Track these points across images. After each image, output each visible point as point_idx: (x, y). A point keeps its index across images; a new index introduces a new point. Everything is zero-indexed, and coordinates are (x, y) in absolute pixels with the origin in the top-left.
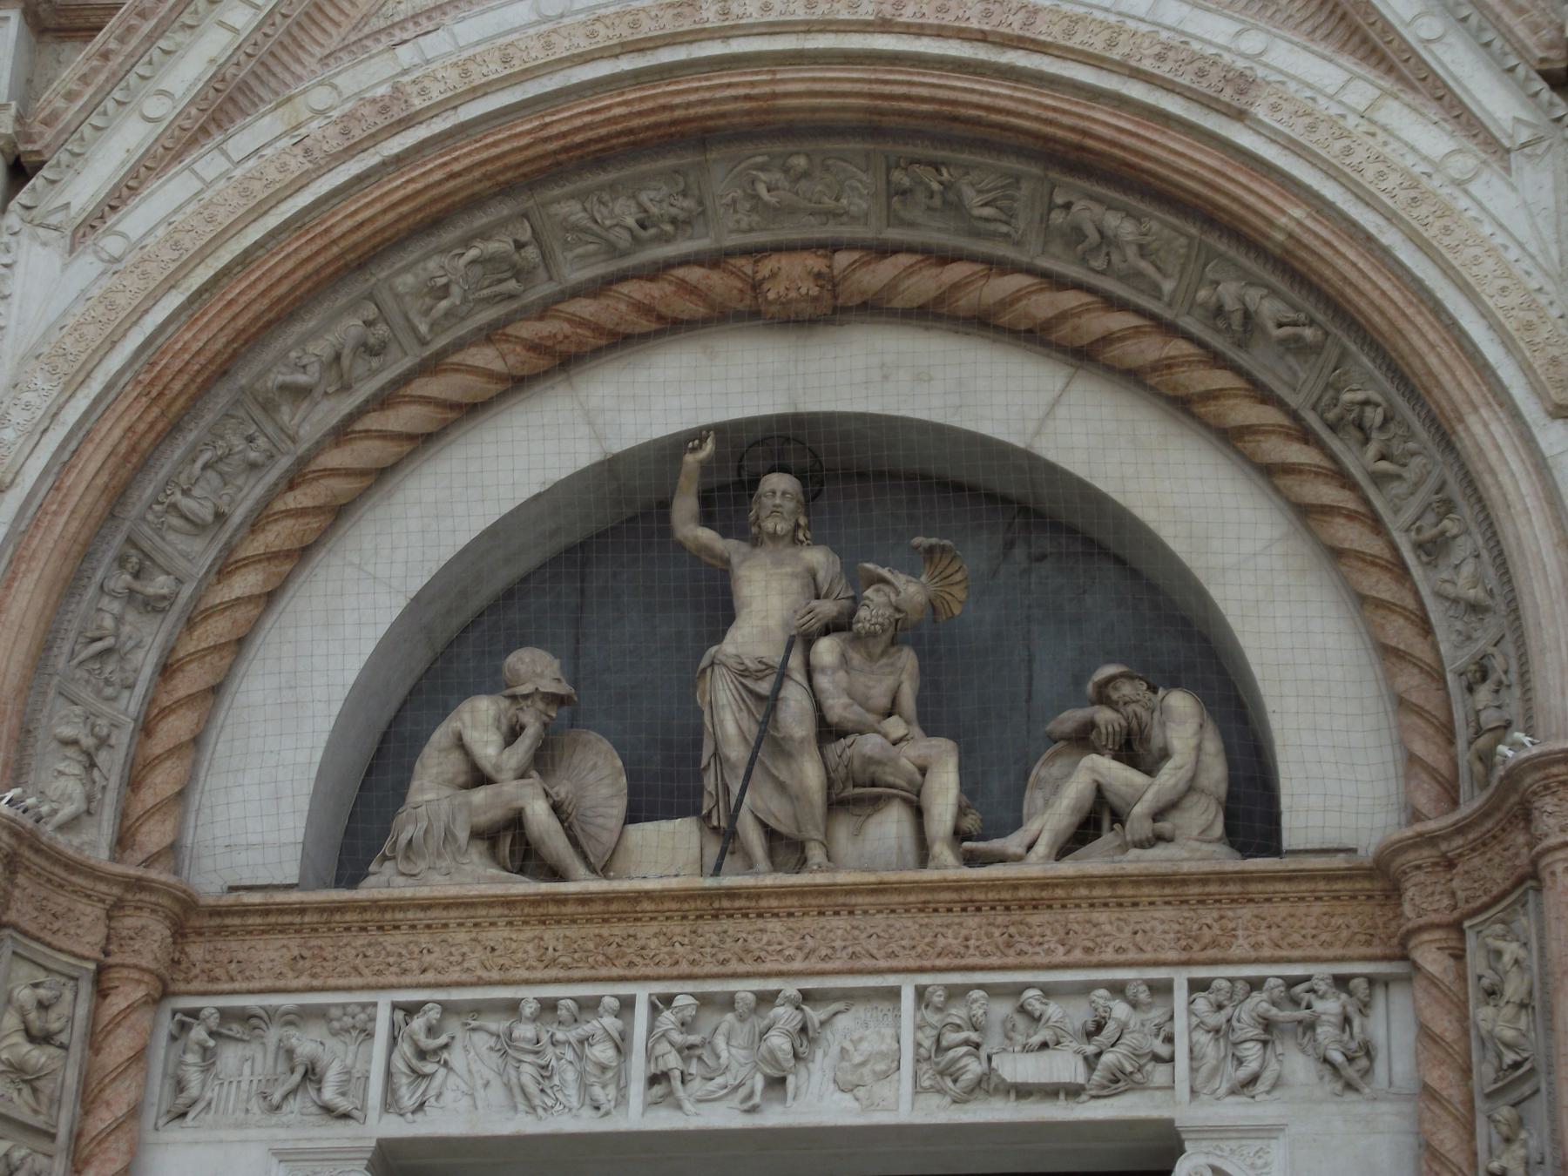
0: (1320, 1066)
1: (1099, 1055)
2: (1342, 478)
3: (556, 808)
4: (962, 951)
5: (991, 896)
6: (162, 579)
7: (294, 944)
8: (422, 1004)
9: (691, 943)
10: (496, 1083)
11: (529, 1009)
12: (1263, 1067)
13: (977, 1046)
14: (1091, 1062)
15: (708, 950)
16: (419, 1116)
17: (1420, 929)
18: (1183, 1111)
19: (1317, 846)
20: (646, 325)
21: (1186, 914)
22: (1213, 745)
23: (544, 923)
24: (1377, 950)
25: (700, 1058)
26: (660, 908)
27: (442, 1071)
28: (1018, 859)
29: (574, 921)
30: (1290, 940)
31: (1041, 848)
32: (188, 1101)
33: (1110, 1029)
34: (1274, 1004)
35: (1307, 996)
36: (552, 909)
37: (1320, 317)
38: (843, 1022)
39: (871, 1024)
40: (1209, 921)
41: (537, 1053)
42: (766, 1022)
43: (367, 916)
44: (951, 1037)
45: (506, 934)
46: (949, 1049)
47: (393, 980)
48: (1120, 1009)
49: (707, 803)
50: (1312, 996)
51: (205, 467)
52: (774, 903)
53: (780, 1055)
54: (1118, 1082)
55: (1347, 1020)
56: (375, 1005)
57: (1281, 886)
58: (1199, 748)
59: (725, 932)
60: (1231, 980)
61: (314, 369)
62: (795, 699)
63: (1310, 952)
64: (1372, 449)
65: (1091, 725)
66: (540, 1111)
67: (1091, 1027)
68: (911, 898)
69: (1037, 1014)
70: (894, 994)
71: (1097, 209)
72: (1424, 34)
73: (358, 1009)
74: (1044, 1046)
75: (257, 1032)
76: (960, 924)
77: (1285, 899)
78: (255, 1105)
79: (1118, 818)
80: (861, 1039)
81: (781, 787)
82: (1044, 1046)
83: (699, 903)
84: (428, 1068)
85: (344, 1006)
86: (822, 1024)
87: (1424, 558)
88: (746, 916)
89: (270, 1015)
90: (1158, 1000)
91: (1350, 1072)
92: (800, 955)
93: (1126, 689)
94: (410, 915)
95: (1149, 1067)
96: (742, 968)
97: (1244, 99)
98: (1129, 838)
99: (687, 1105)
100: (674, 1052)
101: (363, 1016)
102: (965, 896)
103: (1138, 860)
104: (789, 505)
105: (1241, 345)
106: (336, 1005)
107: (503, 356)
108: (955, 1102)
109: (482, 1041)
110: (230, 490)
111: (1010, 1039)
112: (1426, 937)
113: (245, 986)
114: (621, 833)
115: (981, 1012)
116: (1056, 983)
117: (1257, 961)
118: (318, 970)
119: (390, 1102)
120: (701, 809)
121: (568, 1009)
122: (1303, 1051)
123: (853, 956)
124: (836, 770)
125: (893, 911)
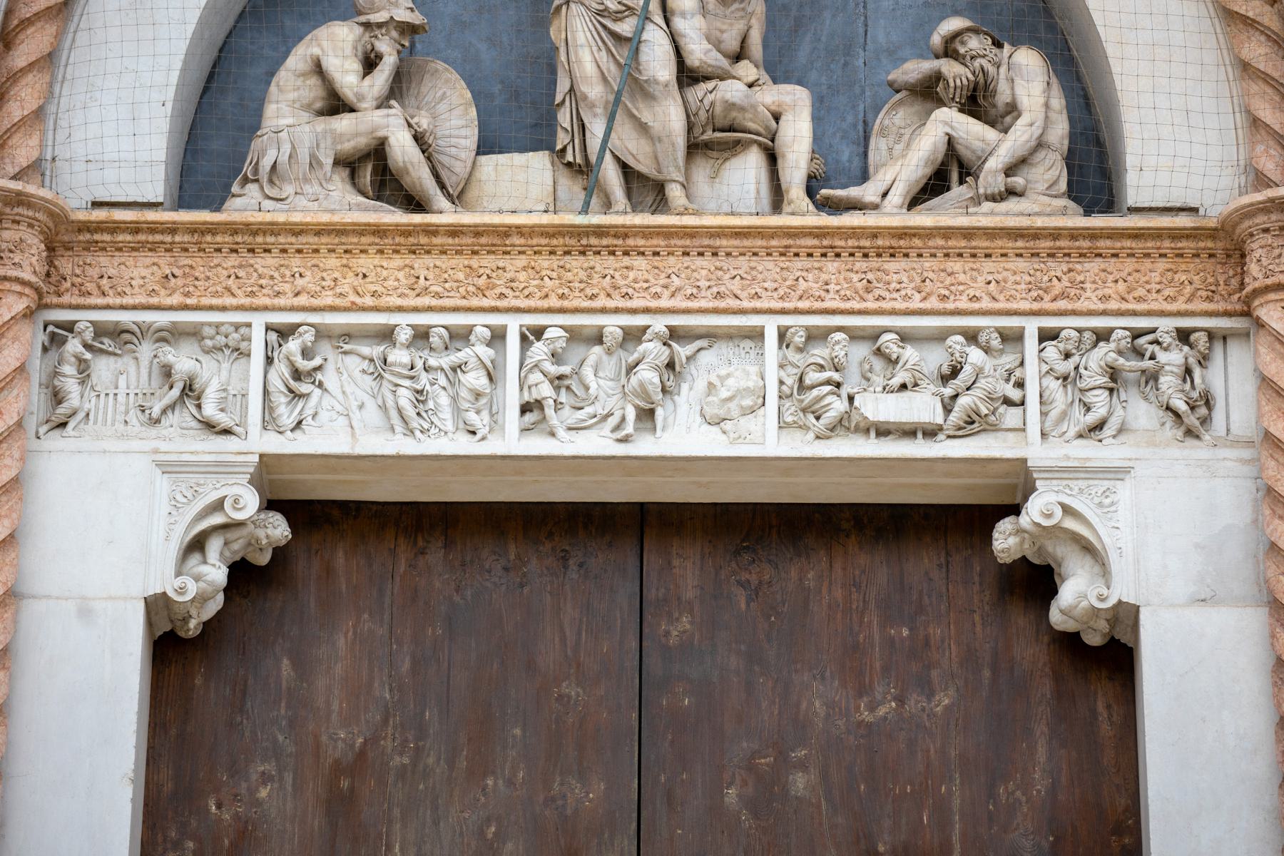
0: (1161, 413)
1: (955, 397)
3: (419, 139)
4: (823, 294)
5: (850, 243)
7: (165, 263)
9: (560, 278)
10: (371, 406)
11: (404, 335)
12: (1110, 414)
13: (838, 385)
15: (577, 285)
16: (298, 433)
18: (1037, 453)
19: (1161, 205)
21: (1036, 266)
22: (1058, 102)
23: (414, 253)
24: (1220, 306)
25: (568, 388)
26: (530, 242)
27: (318, 392)
28: (875, 207)
29: (444, 252)
30: (1136, 294)
31: (896, 197)
32: (69, 412)
33: (966, 375)
34: (1120, 353)
35: (1151, 348)
36: (424, 240)
38: (706, 358)
39: (735, 361)
40: (1059, 274)
41: (412, 378)
42: (636, 356)
43: (239, 239)
44: (812, 377)
45: (376, 262)
46: (813, 387)
47: (267, 301)
49: (562, 139)
50: (1156, 348)
52: (641, 242)
53: (650, 388)
54: (973, 424)
55: (1188, 371)
56: (249, 325)
57: (1128, 243)
58: (1047, 106)
59: (592, 268)
60: (1080, 331)
63: (1155, 306)
65: (938, 77)
66: (418, 433)
67: (946, 370)
68: (774, 243)
69: (894, 357)
70: (756, 335)
73: (232, 329)
74: (904, 387)
75: (129, 346)
76: (820, 269)
77: (1129, 255)
78: (134, 416)
79: (967, 171)
80: (728, 375)
81: (643, 128)
82: (904, 387)
83: (568, 241)
84: (304, 388)
85: (218, 326)
86: (688, 359)
88: (613, 253)
89: (142, 332)
90: (1008, 348)
91: (1192, 420)
92: (667, 293)
93: (974, 43)
94: (281, 239)
95: (1002, 409)
96: (611, 304)
98: (981, 191)
99: (561, 433)
100: (547, 382)
101: (236, 336)
102: (825, 243)
103: (992, 213)
106: (210, 324)
108: (818, 437)
109: (353, 363)
111: (868, 380)
112: (1272, 296)
113: (118, 301)
114: (474, 163)
115: (843, 353)
117: (1104, 313)
118: (191, 289)
119: (269, 420)
121: (441, 337)
122: (1146, 399)
123: (719, 295)
124: (696, 114)
125: (755, 254)
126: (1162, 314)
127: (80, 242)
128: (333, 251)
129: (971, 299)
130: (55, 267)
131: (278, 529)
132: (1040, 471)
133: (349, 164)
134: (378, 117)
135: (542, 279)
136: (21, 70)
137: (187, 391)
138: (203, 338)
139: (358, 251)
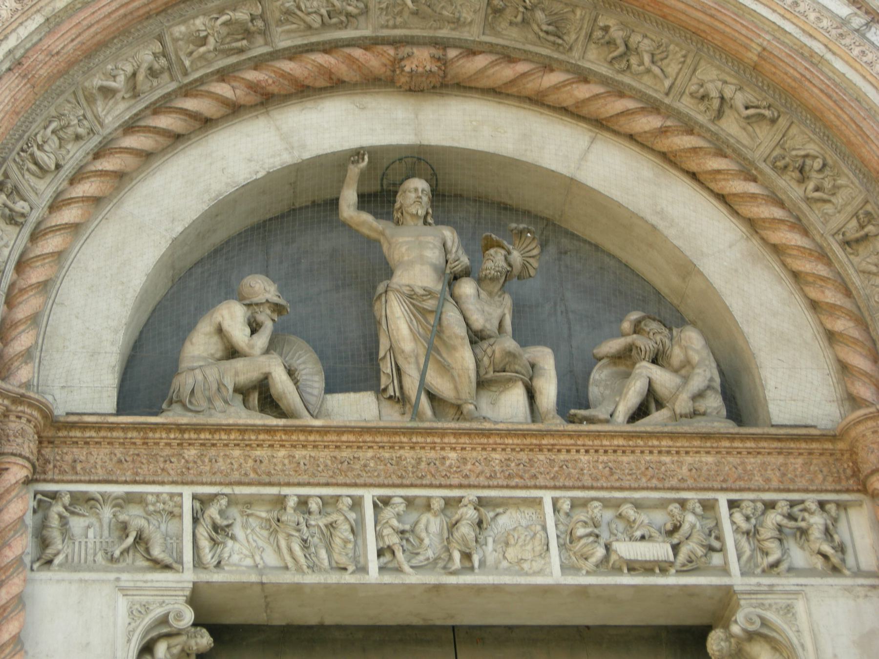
5: (597, 442)
6: (22, 203)
8: (213, 497)
11: (292, 502)
13: (597, 536)
14: (676, 548)
18: (737, 580)
19: (792, 423)
20: (321, 83)
25: (407, 540)
32: (54, 552)
33: (686, 527)
48: (690, 518)
49: (384, 381)
50: (806, 515)
51: (53, 132)
53: (468, 537)
56: (181, 495)
60: (753, 501)
61: (121, 78)
62: (452, 316)
64: (811, 185)
67: (669, 527)
69: (632, 518)
74: (643, 538)
82: (643, 538)
84: (219, 538)
85: (158, 495)
91: (835, 560)
104: (425, 199)
106: (152, 494)
107: (234, 88)
110: (64, 152)
114: (323, 398)
115: (599, 515)
116: (643, 499)
120: (379, 385)
126: (806, 491)
127: (59, 437)
128: (238, 445)
129: (679, 481)
130: (42, 455)
131: (205, 640)
132: (743, 593)
133: (243, 391)
134: (264, 359)
135: (386, 465)
136: (20, 321)
137: (138, 539)
138: (147, 505)
139: (255, 445)
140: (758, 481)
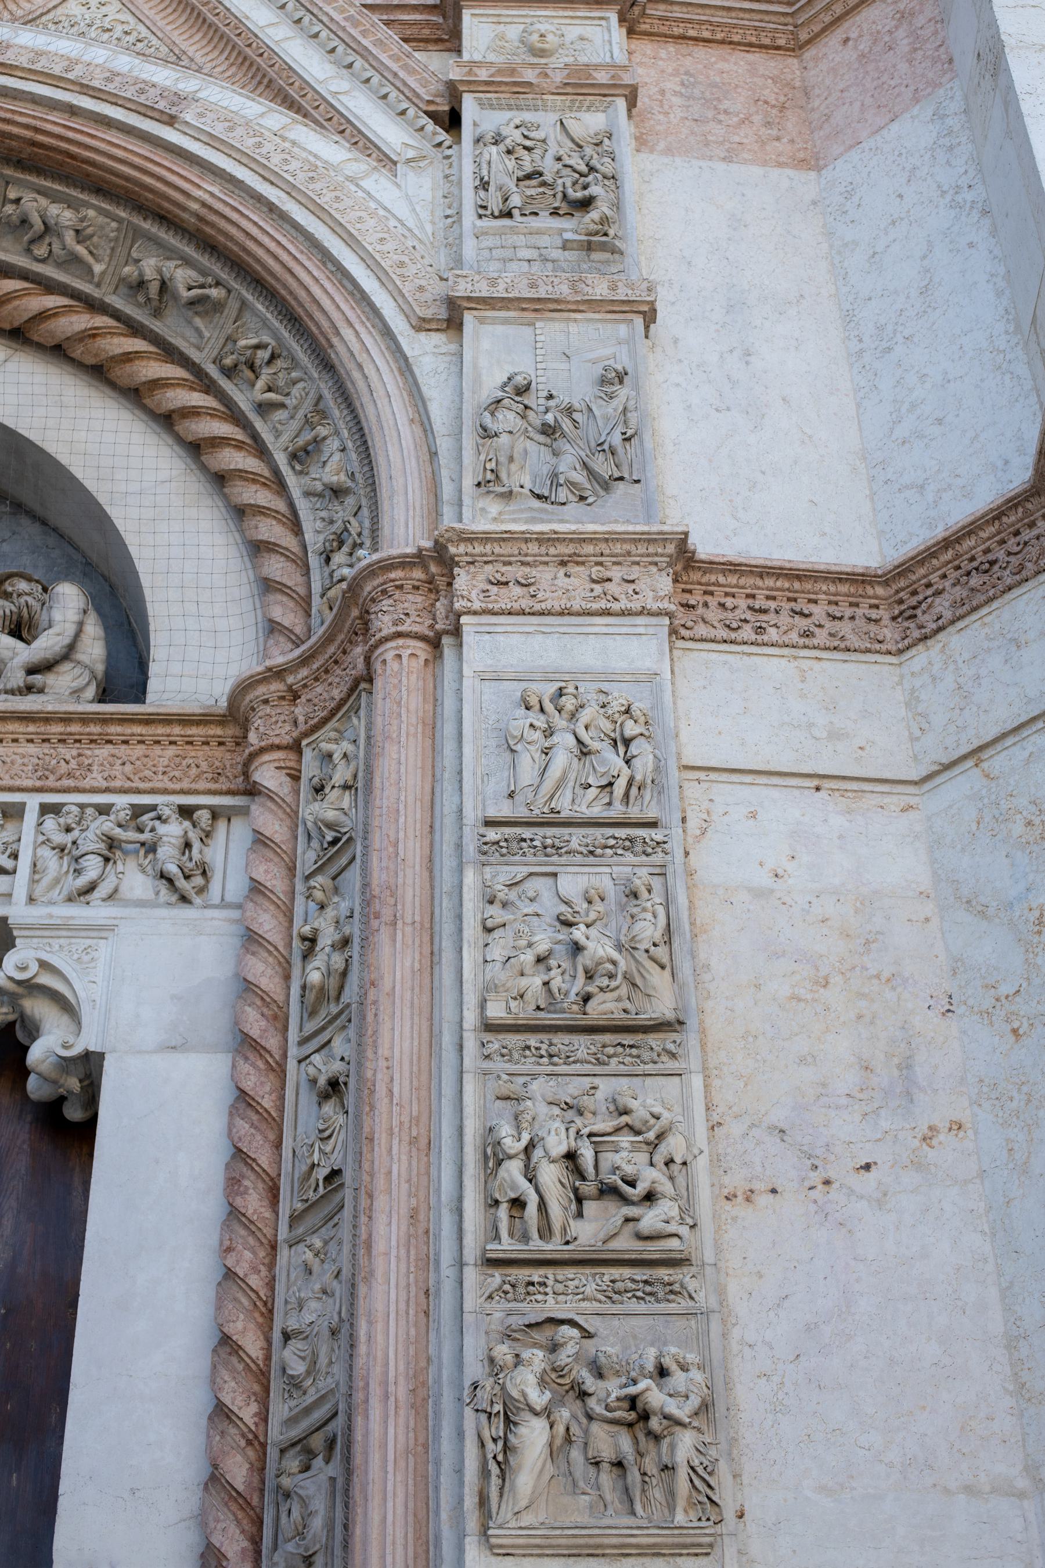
2: (235, 416)
12: (101, 877)
17: (262, 750)
18: (18, 912)
21: (46, 751)
30: (141, 775)
37: (224, 276)
40: (68, 757)
50: (157, 823)
55: (188, 845)
57: (138, 729)
58: (81, 624)
60: (82, 806)
63: (159, 785)
71: (43, 201)
72: (333, 88)
77: (140, 742)
87: (298, 467)
97: (174, 109)
105: (157, 313)
112: (266, 757)
117: (107, 790)
126: (165, 792)
140: (96, 779)
